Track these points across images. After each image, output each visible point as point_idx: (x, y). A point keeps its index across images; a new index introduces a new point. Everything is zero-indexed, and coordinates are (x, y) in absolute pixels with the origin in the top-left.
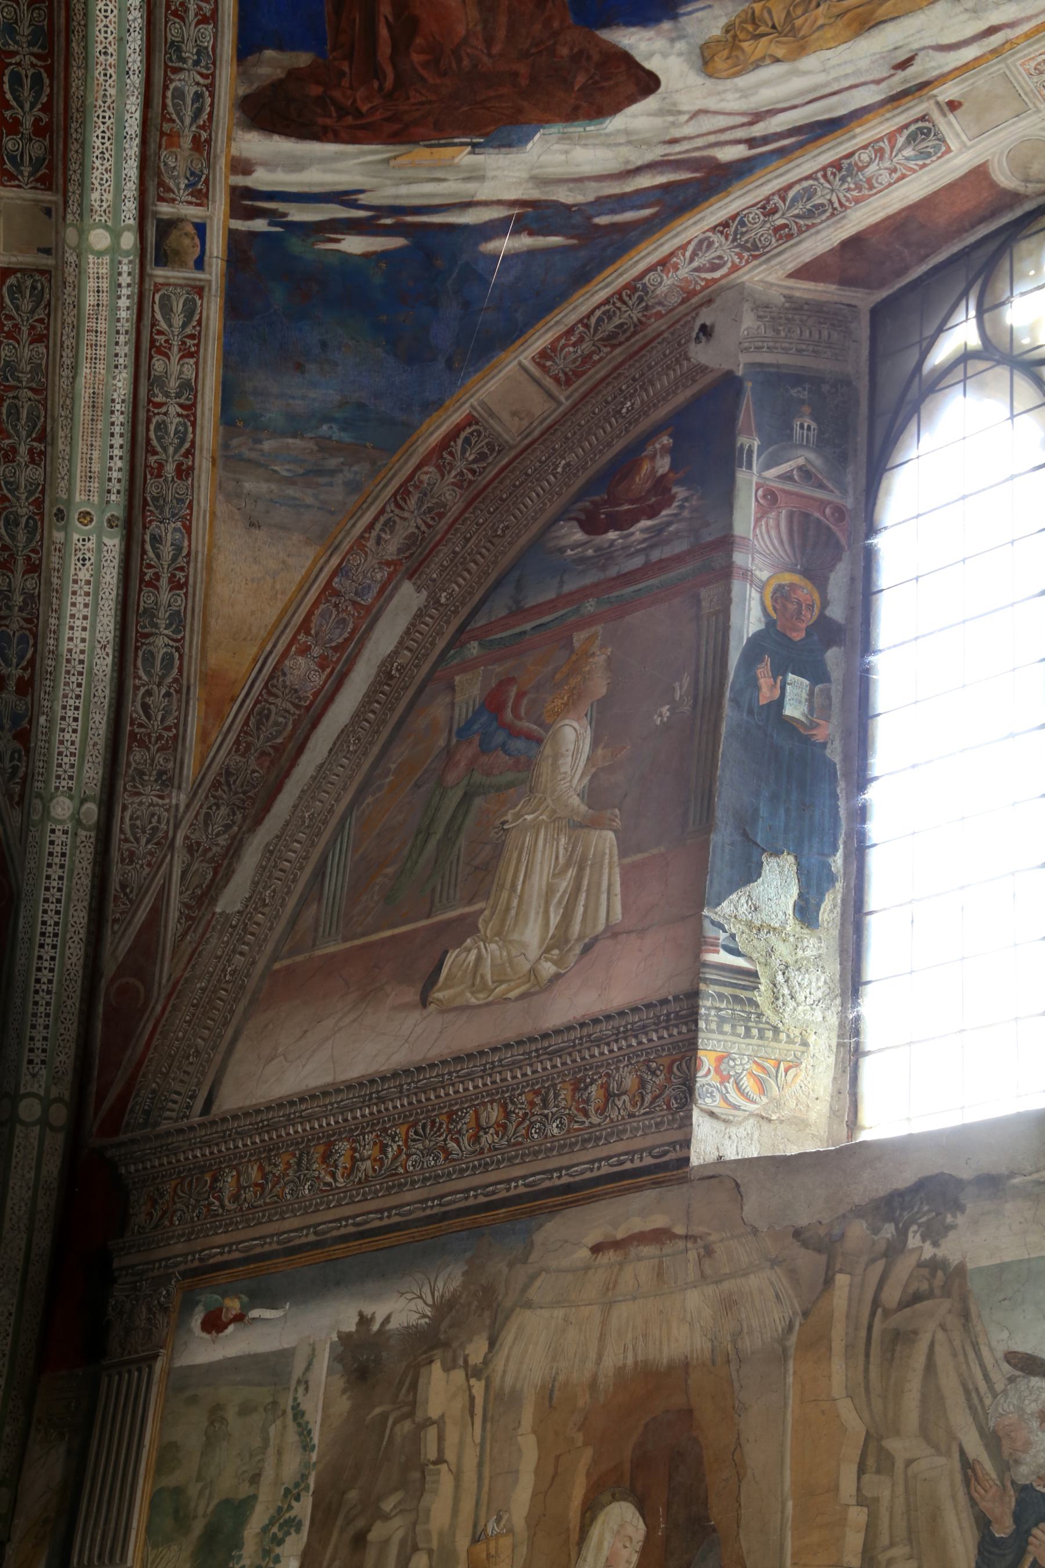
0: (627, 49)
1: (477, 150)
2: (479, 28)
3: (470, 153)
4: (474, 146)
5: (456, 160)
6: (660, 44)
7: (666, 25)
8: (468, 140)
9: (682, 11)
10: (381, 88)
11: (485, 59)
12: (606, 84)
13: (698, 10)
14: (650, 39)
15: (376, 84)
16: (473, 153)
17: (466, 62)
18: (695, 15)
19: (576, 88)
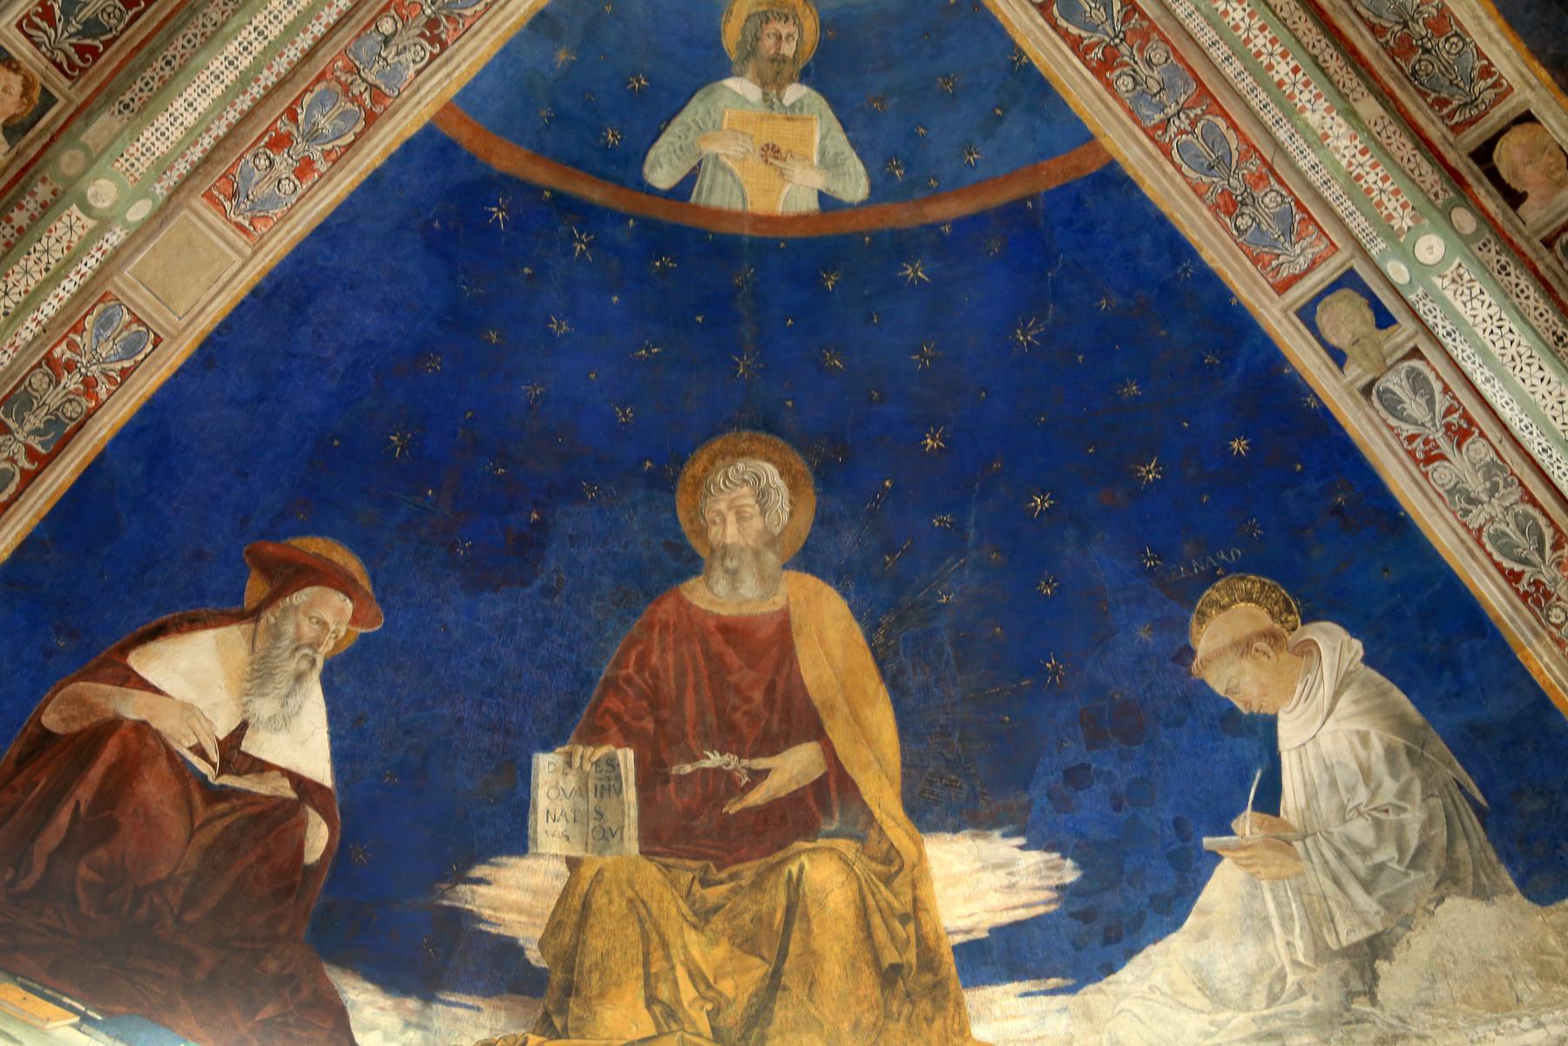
0: (348, 1005)
1: (85, 1027)
2: (187, 880)
3: (73, 1025)
4: (85, 1019)
5: (50, 1026)
6: (391, 1020)
7: (412, 1004)
8: (83, 1009)
9: (441, 997)
10: (13, 882)
11: (170, 921)
12: (296, 1032)
13: (461, 1005)
14: (382, 1009)
15: (9, 875)
16: (77, 1027)
17: (143, 911)
18: (454, 1010)
19: (258, 1018)
